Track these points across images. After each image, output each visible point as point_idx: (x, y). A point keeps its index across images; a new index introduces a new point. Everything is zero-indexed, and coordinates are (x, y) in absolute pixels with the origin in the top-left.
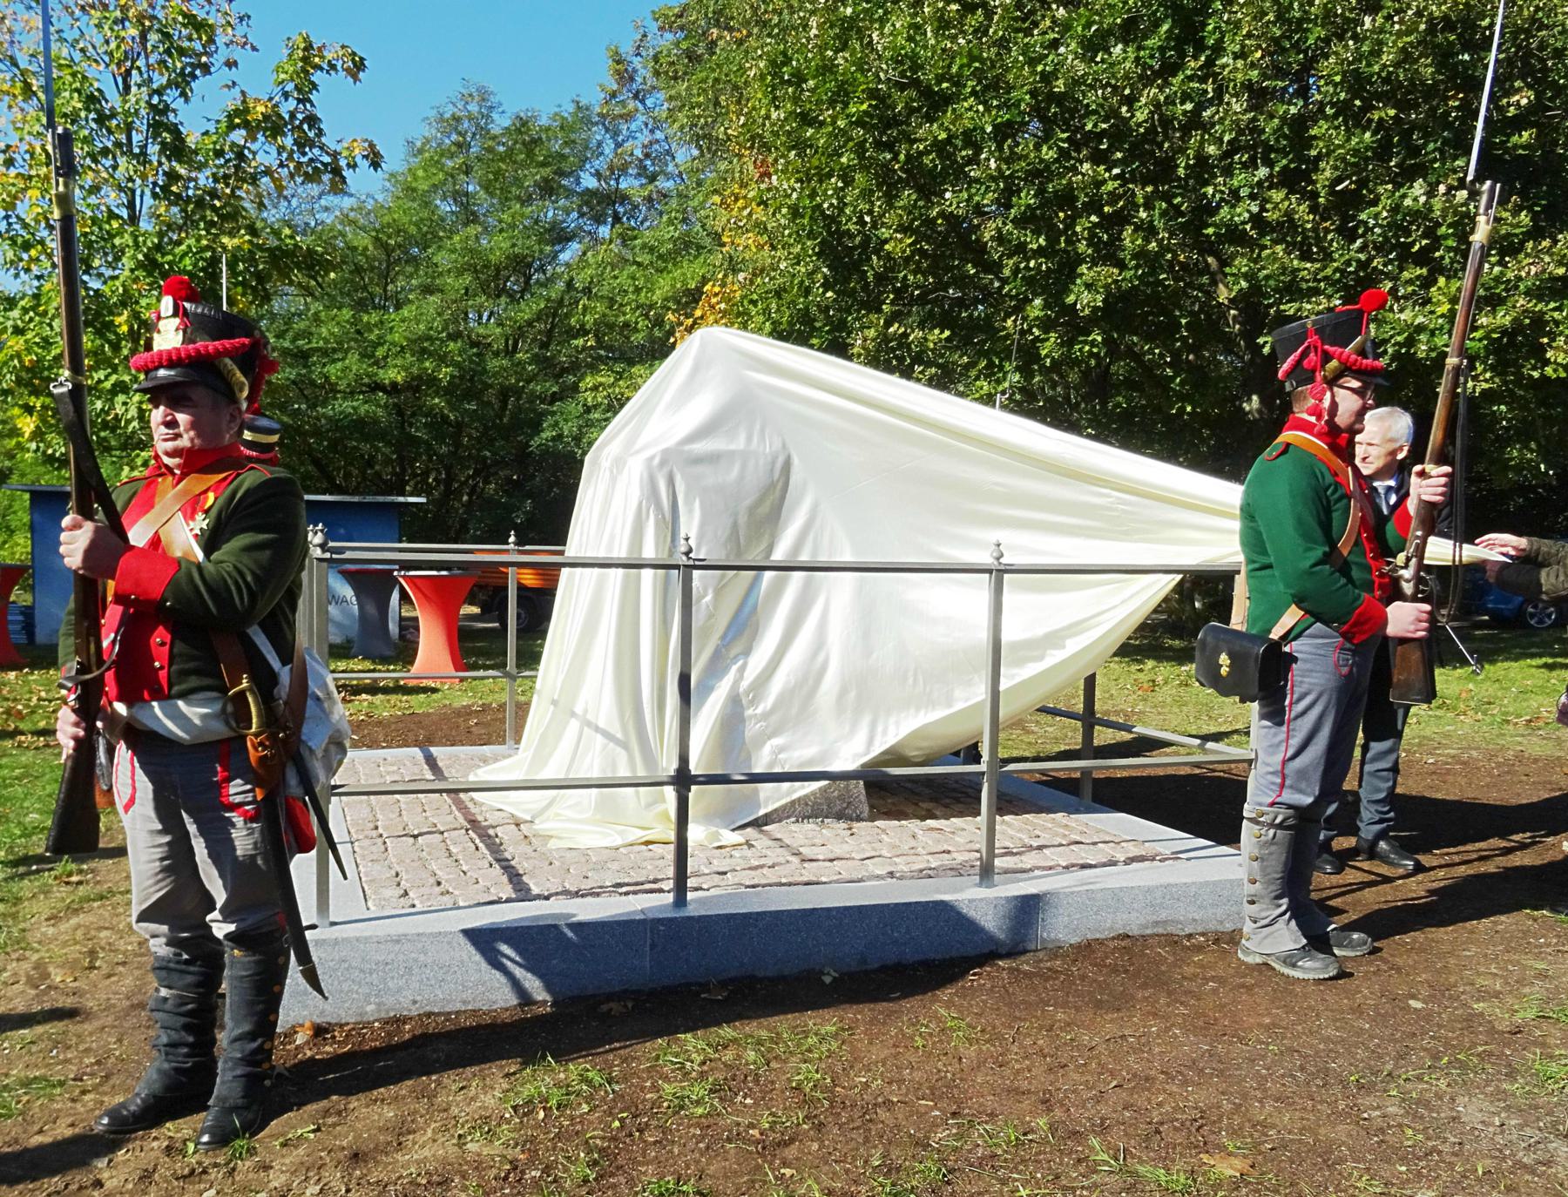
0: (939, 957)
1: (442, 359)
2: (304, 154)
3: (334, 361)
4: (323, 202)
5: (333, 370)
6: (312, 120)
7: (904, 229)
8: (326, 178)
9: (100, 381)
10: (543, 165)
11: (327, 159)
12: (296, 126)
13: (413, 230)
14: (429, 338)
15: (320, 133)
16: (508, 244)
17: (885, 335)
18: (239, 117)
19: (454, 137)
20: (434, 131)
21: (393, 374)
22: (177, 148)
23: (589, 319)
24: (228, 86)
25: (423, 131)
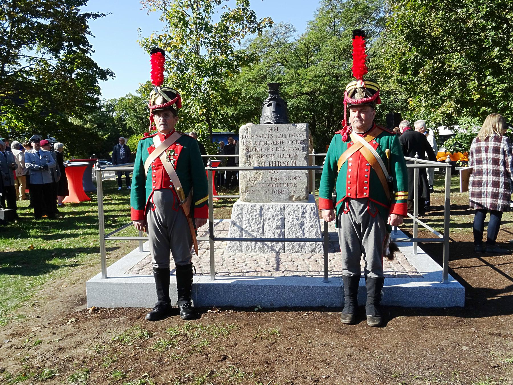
0: (302, 306)
1: (322, 83)
2: (250, 25)
3: (288, 87)
4: (287, 34)
5: (287, 90)
6: (252, 14)
7: (441, 26)
8: (257, 31)
9: (189, 103)
10: (360, 12)
11: (256, 26)
12: (244, 16)
13: (316, 40)
14: (319, 76)
15: (255, 17)
16: (346, 42)
17: (433, 67)
18: (226, 17)
19: (330, 7)
20: (323, 6)
21: (306, 89)
22: (208, 30)
23: (374, 65)
24: (224, 7)
25: (320, 6)
